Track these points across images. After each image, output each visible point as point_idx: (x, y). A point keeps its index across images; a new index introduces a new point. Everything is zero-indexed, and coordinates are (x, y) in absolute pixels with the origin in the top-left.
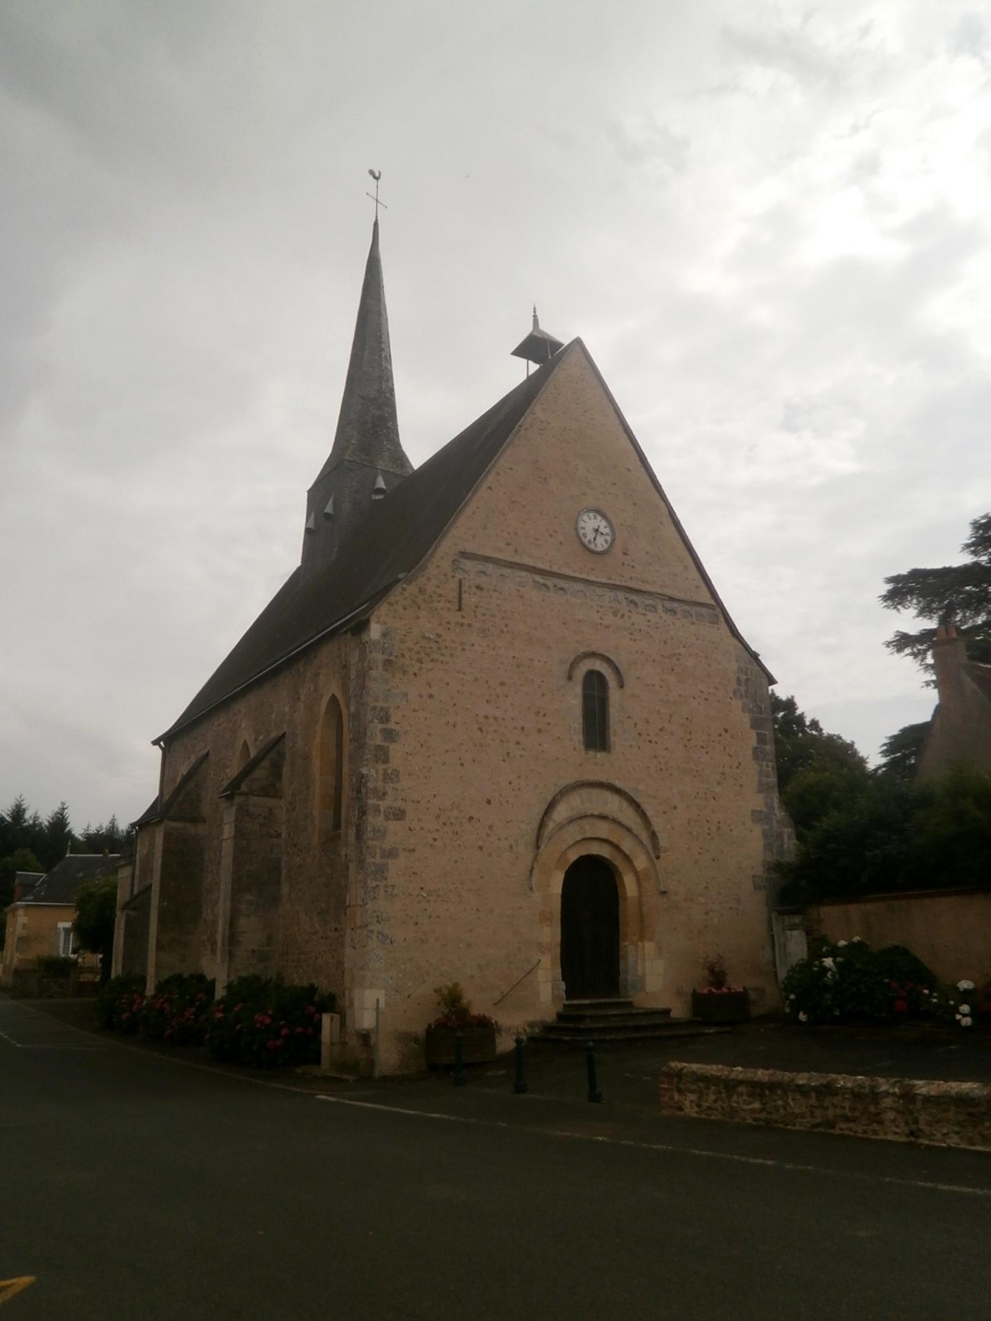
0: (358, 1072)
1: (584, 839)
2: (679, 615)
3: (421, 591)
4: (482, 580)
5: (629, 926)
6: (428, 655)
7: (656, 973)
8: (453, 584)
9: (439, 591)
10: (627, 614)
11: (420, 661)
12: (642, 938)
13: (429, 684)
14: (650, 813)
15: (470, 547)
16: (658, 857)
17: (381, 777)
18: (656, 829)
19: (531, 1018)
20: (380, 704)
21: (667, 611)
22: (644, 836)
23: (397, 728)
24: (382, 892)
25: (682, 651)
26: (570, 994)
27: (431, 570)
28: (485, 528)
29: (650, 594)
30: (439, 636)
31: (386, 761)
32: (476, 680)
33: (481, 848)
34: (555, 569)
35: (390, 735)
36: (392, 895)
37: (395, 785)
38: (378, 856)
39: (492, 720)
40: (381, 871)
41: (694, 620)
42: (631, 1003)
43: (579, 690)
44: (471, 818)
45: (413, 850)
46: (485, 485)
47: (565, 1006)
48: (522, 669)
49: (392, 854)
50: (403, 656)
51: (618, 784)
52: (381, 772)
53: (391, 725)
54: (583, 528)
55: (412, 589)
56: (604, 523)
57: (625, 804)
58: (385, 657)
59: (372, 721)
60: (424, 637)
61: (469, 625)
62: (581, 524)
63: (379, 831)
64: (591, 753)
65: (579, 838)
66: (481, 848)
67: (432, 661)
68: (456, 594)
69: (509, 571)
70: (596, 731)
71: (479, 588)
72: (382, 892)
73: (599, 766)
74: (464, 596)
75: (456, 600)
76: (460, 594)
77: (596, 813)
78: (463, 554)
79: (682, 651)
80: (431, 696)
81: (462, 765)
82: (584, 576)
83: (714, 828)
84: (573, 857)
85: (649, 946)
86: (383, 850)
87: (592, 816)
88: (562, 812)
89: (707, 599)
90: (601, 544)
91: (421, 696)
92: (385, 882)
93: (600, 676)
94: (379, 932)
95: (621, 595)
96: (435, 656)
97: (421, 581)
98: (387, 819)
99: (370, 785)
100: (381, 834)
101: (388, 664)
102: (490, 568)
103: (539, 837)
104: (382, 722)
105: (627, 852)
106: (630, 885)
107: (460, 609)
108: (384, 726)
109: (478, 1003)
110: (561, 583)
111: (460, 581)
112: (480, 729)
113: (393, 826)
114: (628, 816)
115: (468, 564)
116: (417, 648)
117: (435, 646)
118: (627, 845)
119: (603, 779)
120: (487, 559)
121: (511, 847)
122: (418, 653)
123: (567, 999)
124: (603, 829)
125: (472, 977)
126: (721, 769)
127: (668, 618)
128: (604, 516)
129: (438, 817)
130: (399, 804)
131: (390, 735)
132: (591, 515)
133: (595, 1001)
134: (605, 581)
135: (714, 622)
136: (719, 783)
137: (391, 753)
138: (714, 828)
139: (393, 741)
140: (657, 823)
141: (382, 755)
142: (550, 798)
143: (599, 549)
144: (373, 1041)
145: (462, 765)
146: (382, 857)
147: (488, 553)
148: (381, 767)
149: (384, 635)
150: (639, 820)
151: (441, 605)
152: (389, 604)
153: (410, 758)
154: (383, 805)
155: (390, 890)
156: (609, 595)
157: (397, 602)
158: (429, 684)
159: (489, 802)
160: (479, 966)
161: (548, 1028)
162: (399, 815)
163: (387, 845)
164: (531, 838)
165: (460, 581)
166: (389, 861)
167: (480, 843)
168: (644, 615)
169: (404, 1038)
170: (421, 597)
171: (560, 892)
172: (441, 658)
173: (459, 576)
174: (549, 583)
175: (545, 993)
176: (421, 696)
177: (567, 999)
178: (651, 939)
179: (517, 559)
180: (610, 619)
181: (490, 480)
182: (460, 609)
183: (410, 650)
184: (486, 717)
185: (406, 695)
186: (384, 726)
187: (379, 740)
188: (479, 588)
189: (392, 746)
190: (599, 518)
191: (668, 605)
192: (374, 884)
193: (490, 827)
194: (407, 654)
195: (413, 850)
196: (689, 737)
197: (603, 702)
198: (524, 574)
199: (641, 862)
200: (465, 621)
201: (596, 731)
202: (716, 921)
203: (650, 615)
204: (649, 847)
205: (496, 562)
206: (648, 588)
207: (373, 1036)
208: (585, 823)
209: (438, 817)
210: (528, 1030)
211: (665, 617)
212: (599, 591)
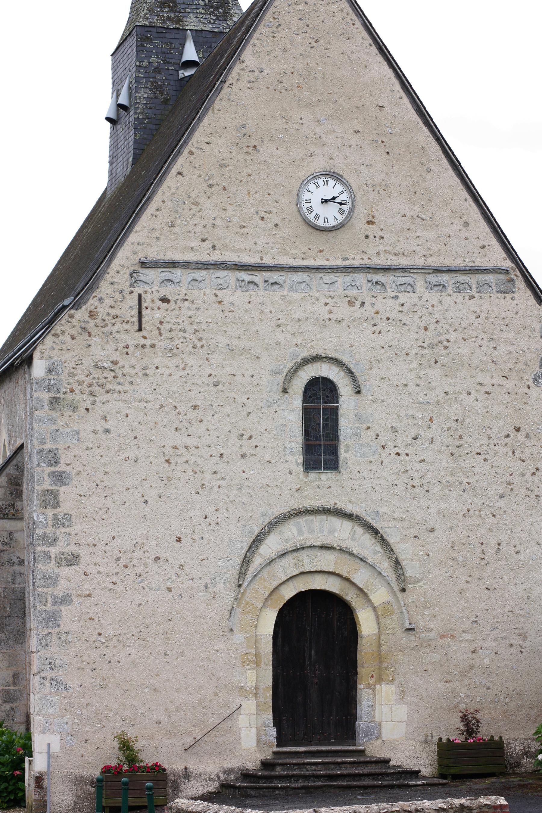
0: (392, 780)
1: (302, 573)
2: (450, 291)
3: (92, 315)
4: (167, 291)
5: (366, 666)
6: (102, 386)
7: (395, 720)
8: (133, 301)
9: (113, 312)
10: (368, 300)
11: (92, 394)
12: (380, 680)
13: (105, 419)
14: (392, 540)
15: (153, 254)
16: (403, 590)
17: (51, 522)
18: (401, 558)
19: (228, 765)
20: (47, 447)
21: (432, 286)
22: (385, 566)
23: (68, 469)
24: (54, 638)
25: (452, 336)
26: (281, 741)
27: (105, 288)
28: (173, 226)
29: (404, 269)
30: (115, 363)
31: (57, 505)
32: (162, 406)
33: (169, 589)
34: (268, 260)
35: (60, 478)
36: (66, 642)
37: (67, 530)
38: (49, 605)
39: (183, 451)
40: (52, 619)
41: (474, 292)
42: (363, 751)
43: (297, 402)
44: (157, 559)
45: (90, 595)
46: (174, 170)
47: (275, 753)
48: (220, 387)
49: (66, 600)
50: (72, 391)
51: (349, 508)
52: (50, 517)
53: (61, 467)
54: (308, 201)
55: (81, 314)
56: (339, 188)
57: (360, 530)
58: (52, 395)
59: (38, 465)
60: (97, 367)
61: (153, 346)
62: (306, 196)
63: (50, 578)
64: (313, 475)
65: (267, 593)
66: (169, 589)
67: (107, 392)
68: (135, 312)
69: (204, 273)
70: (321, 445)
71: (165, 300)
72: (54, 638)
73: (324, 489)
74: (144, 312)
75: (136, 319)
76: (140, 313)
77: (319, 543)
78: (143, 264)
79: (452, 336)
80: (107, 431)
81: (146, 502)
82: (310, 263)
83: (490, 551)
84: (289, 592)
85: (386, 690)
86: (55, 597)
87: (312, 547)
88: (272, 545)
89: (497, 258)
90: (330, 215)
91: (95, 432)
92: (57, 630)
93: (327, 381)
94: (52, 679)
95: (361, 278)
96: (109, 386)
97: (92, 303)
98: (59, 565)
99: (39, 532)
100: (51, 580)
101: (55, 401)
102: (178, 274)
103: (242, 574)
104: (50, 464)
105: (361, 586)
106: (366, 623)
107: (140, 329)
108: (53, 469)
109: (156, 750)
110: (275, 276)
111: (140, 296)
112: (168, 461)
113: (65, 571)
114: (364, 544)
115: (150, 274)
116: (89, 380)
117: (110, 375)
118: (361, 577)
119: (328, 503)
120: (174, 264)
121: (206, 586)
122: (90, 385)
123: (278, 746)
124: (327, 561)
125: (158, 722)
126: (507, 478)
127: (433, 296)
128: (338, 178)
129: (118, 559)
130: (72, 549)
131: (60, 478)
132: (320, 181)
133: (312, 748)
134: (340, 263)
135: (507, 289)
136: (502, 496)
137: (62, 497)
138: (490, 551)
139: (64, 483)
140: (404, 550)
141: (51, 499)
142: (257, 531)
143: (332, 223)
144: (45, 783)
145: (146, 502)
146: (54, 605)
147: (178, 257)
148: (50, 512)
149: (50, 371)
150: (378, 548)
151: (116, 328)
152: (56, 335)
153: (83, 500)
154: (54, 551)
155: (63, 636)
156: (342, 280)
157: (63, 332)
158: (105, 419)
159: (179, 540)
160: (166, 711)
161: (246, 776)
162: (73, 560)
163: (59, 591)
164: (232, 575)
165: (140, 296)
166: (63, 608)
167: (169, 584)
168: (396, 298)
169: (79, 781)
170: (92, 322)
171: (271, 632)
172: (118, 388)
173: (138, 290)
174: (256, 279)
175: (250, 735)
176: (95, 432)
177: (278, 746)
178: (391, 682)
179: (216, 257)
180: (343, 311)
181: (181, 163)
182: (140, 329)
183: (80, 383)
184: (175, 448)
185: (78, 433)
186: (53, 469)
187: (47, 485)
188: (165, 300)
189: (63, 489)
190: (332, 182)
191: (433, 279)
192: (46, 631)
193: (181, 567)
194: (77, 390)
195: (90, 595)
196: (458, 443)
197: (333, 416)
198: (222, 273)
199: (380, 595)
200: (148, 342)
201: (321, 445)
202: (487, 661)
203: (403, 297)
204: (392, 578)
205: (185, 265)
206: (404, 262)
207: (45, 778)
208: (304, 555)
209: (118, 559)
210: (222, 776)
211: (427, 295)
212: (328, 278)
